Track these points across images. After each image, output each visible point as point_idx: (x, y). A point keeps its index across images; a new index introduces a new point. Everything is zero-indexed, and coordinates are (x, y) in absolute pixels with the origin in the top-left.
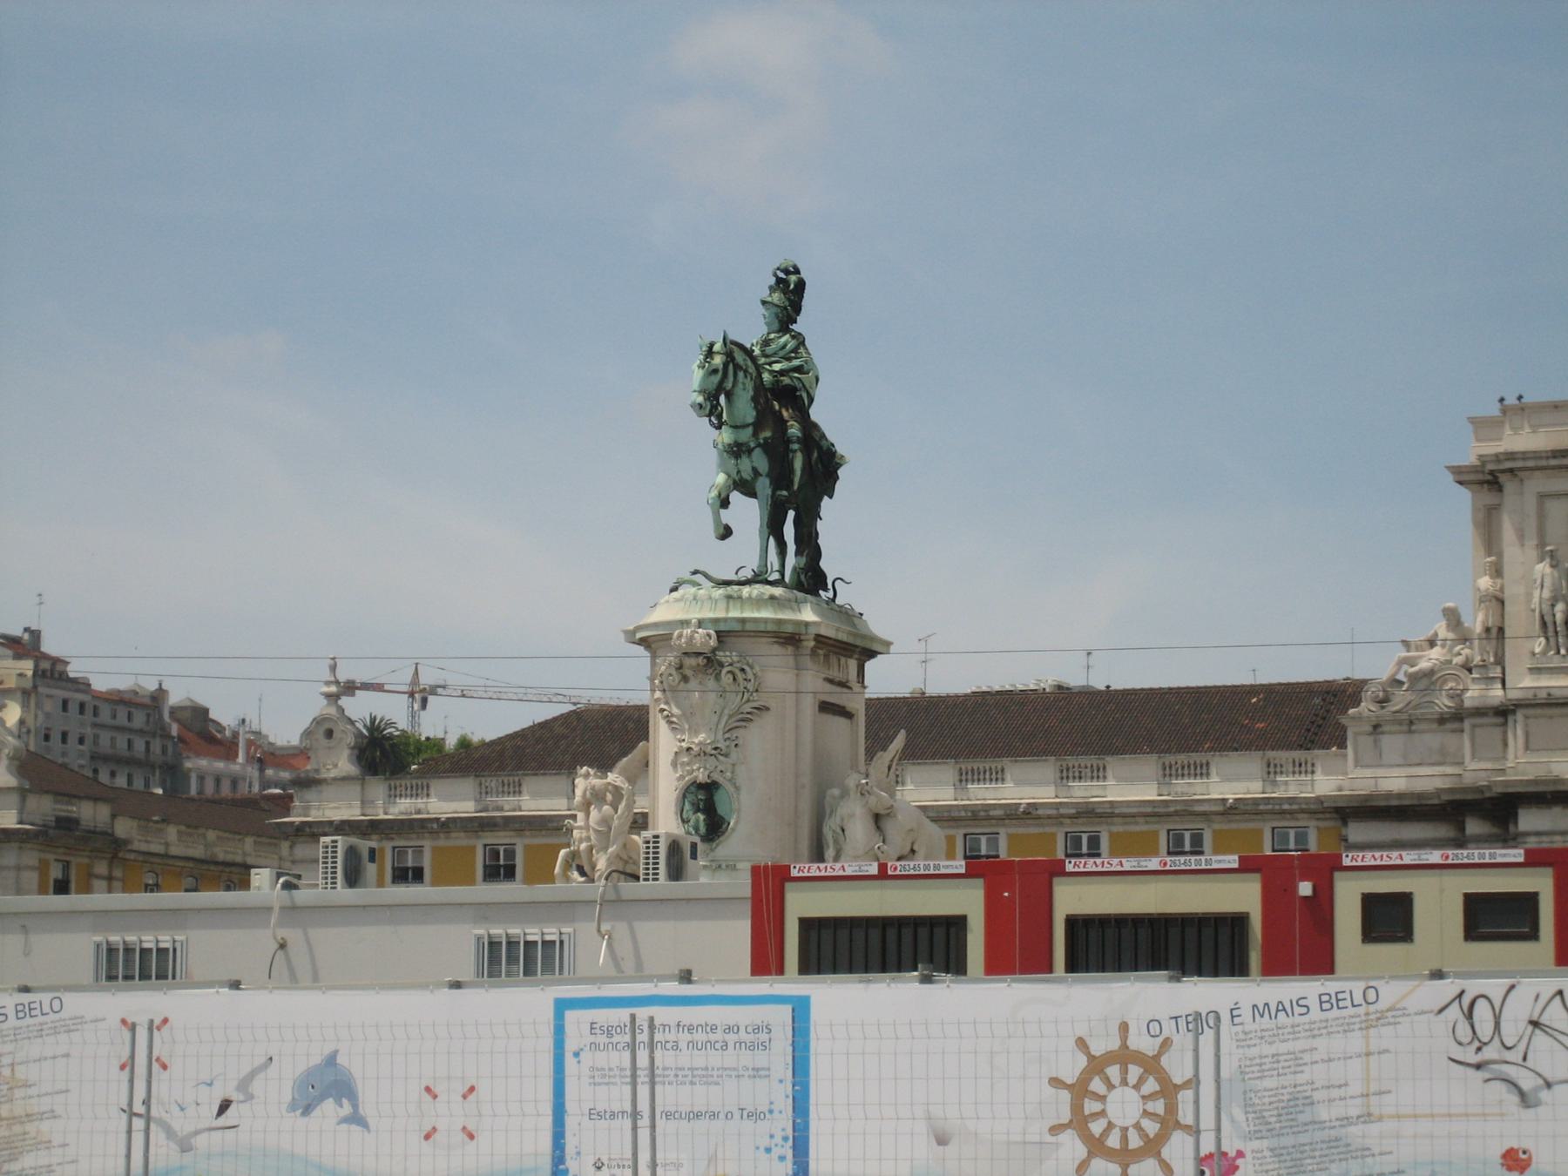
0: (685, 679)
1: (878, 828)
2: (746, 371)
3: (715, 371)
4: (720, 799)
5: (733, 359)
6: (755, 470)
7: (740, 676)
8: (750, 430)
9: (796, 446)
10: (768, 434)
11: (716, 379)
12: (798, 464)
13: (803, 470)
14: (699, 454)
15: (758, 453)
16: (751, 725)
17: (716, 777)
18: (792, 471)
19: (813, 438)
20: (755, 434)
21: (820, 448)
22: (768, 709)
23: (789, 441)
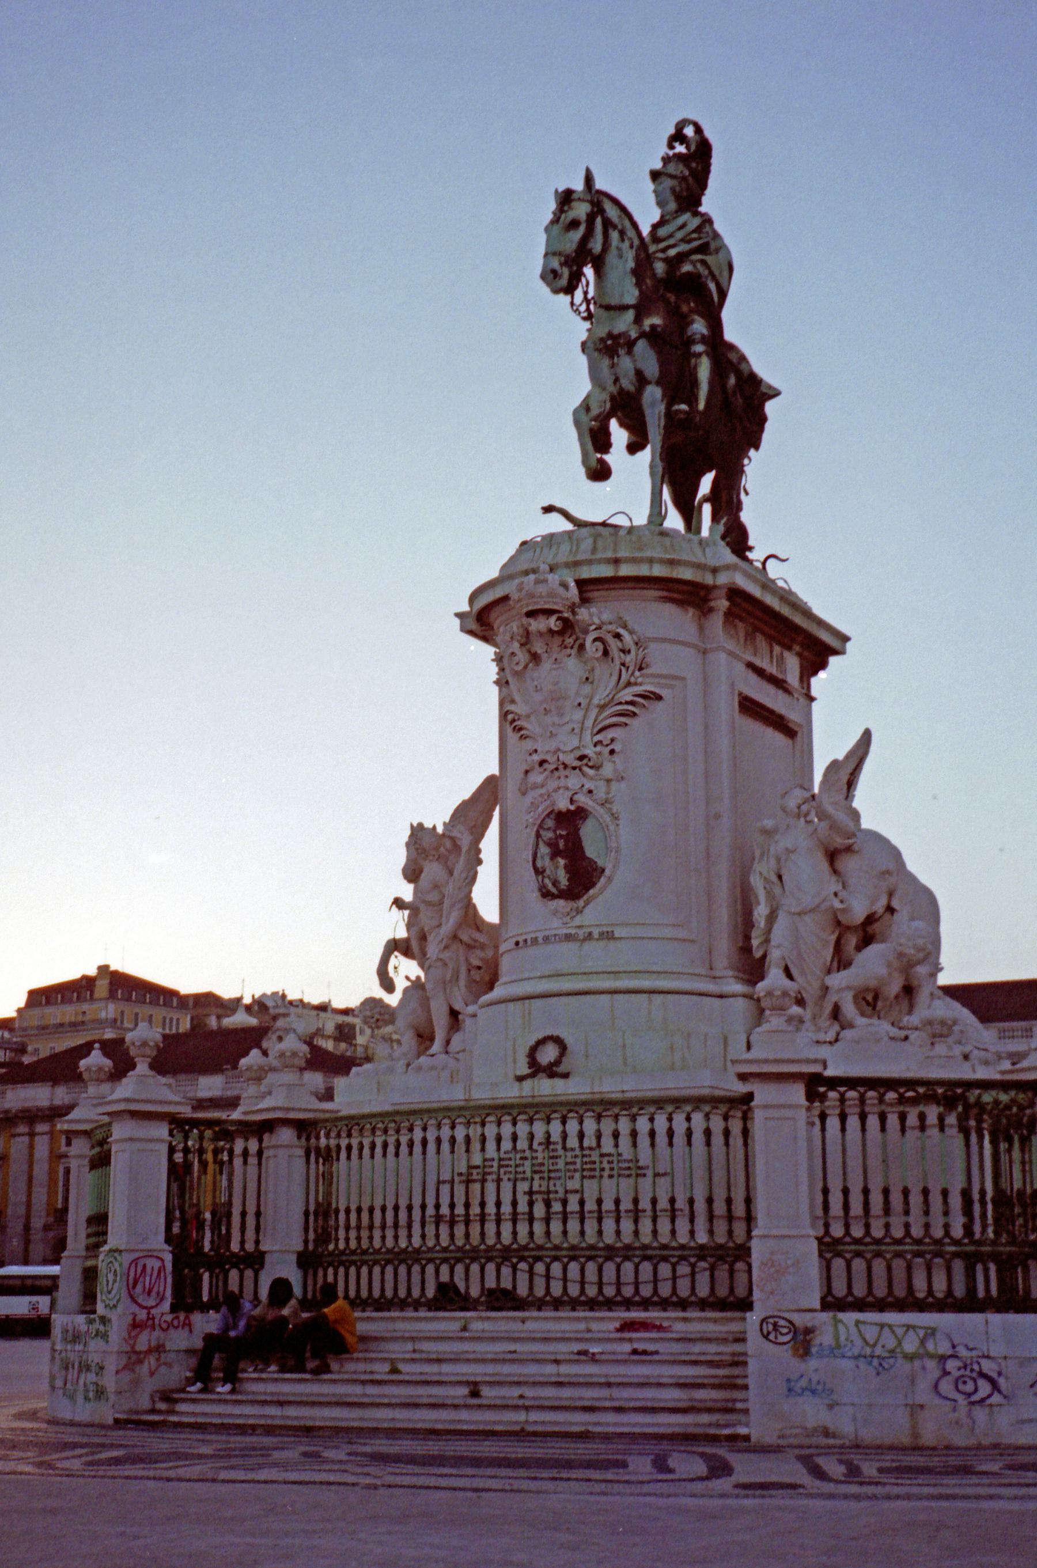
0: (535, 658)
1: (835, 871)
2: (622, 233)
3: (574, 224)
4: (588, 833)
5: (602, 211)
6: (639, 373)
7: (614, 645)
8: (630, 315)
9: (699, 348)
10: (657, 320)
11: (577, 235)
12: (704, 371)
13: (711, 383)
14: (553, 354)
15: (641, 346)
16: (633, 722)
17: (582, 799)
18: (695, 383)
19: (726, 358)
20: (638, 320)
21: (739, 374)
22: (659, 698)
23: (691, 341)
